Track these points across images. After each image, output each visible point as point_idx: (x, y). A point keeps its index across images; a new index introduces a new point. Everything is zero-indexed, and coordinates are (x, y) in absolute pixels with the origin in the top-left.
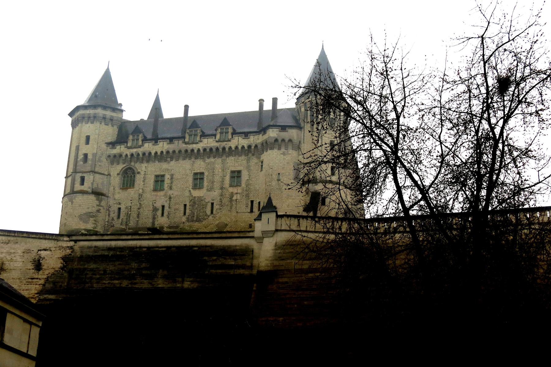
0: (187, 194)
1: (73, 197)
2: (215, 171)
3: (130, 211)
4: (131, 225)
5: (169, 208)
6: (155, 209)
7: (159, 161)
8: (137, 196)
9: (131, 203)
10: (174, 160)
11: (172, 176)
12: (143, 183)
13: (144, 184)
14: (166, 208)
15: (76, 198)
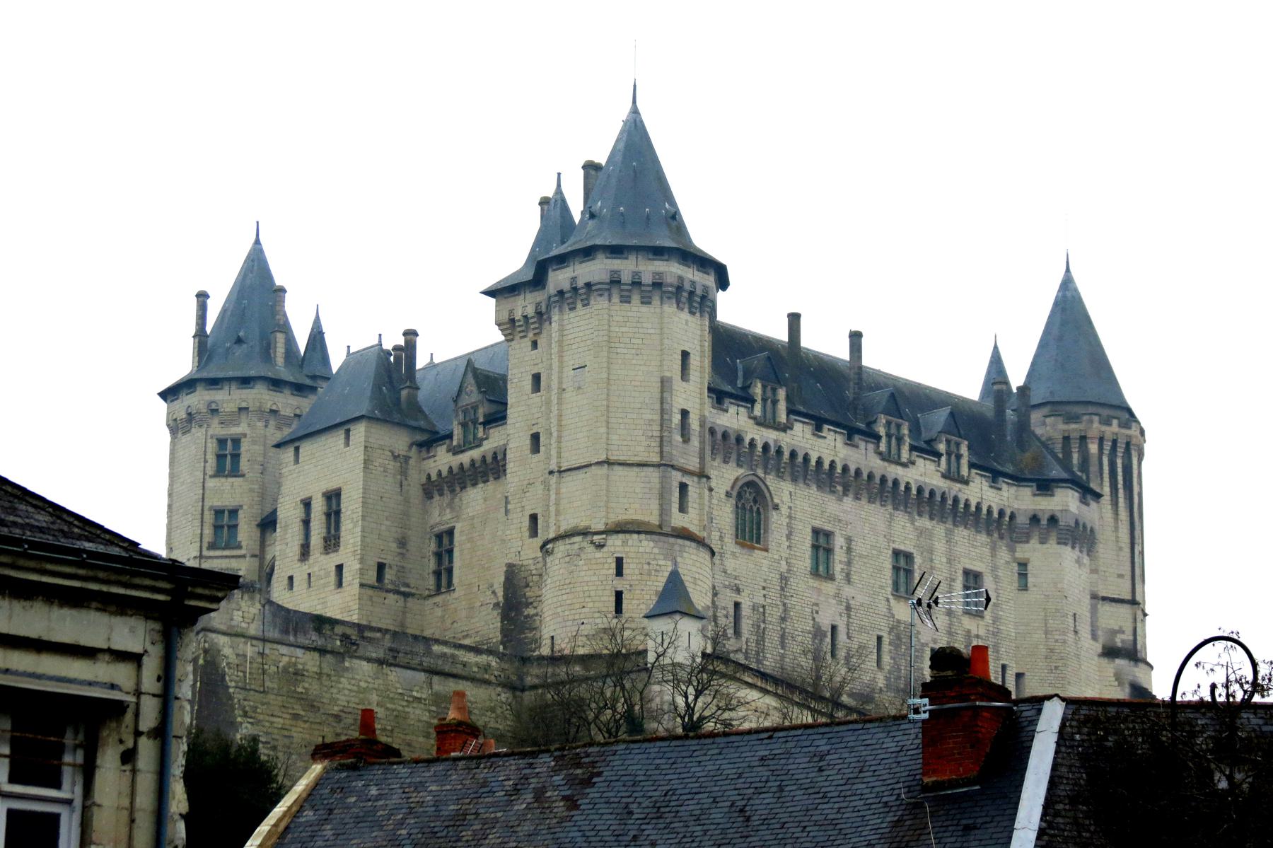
0: (882, 608)
1: (677, 548)
2: (934, 557)
3: (764, 622)
4: (768, 663)
5: (849, 637)
6: (818, 633)
7: (819, 487)
8: (775, 577)
9: (764, 596)
10: (851, 496)
11: (849, 540)
12: (787, 544)
13: (789, 547)
14: (842, 637)
15: (685, 555)
